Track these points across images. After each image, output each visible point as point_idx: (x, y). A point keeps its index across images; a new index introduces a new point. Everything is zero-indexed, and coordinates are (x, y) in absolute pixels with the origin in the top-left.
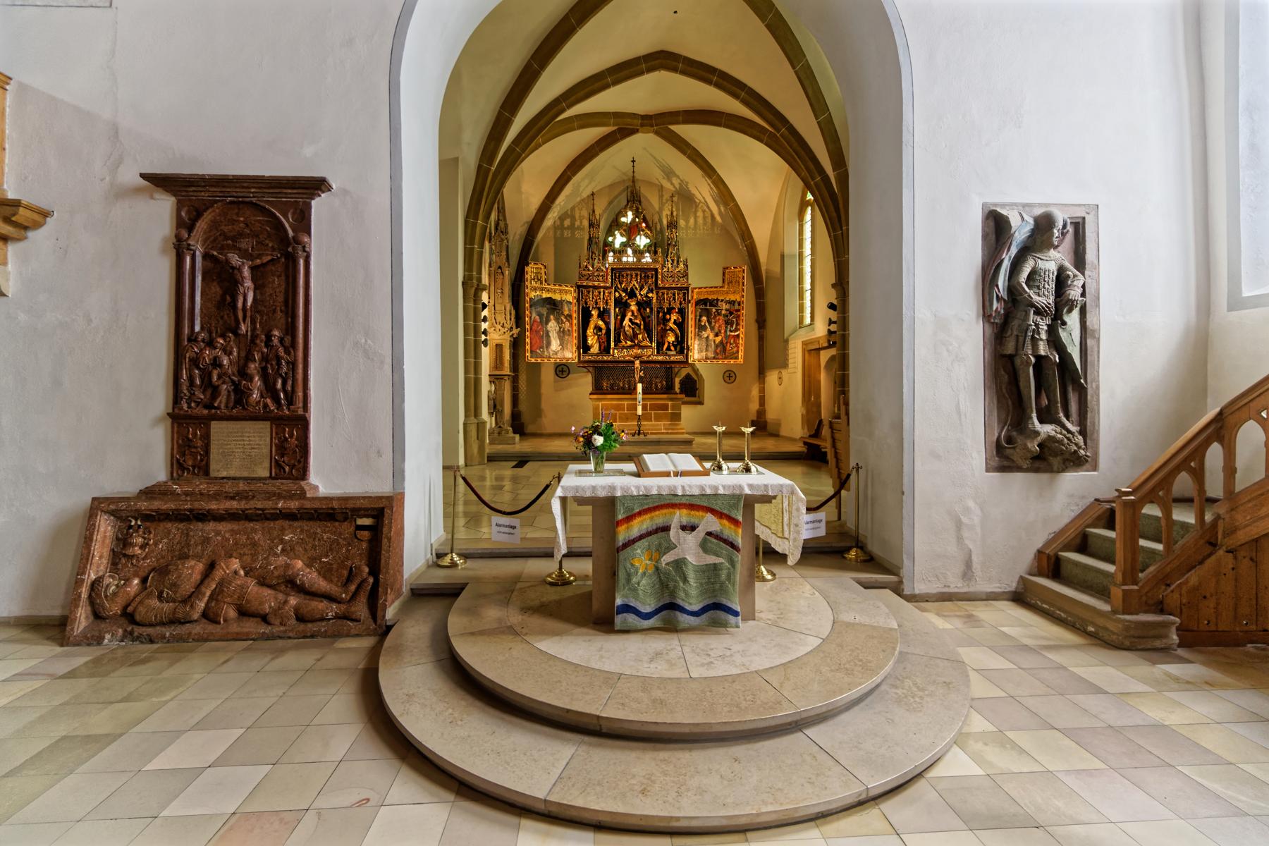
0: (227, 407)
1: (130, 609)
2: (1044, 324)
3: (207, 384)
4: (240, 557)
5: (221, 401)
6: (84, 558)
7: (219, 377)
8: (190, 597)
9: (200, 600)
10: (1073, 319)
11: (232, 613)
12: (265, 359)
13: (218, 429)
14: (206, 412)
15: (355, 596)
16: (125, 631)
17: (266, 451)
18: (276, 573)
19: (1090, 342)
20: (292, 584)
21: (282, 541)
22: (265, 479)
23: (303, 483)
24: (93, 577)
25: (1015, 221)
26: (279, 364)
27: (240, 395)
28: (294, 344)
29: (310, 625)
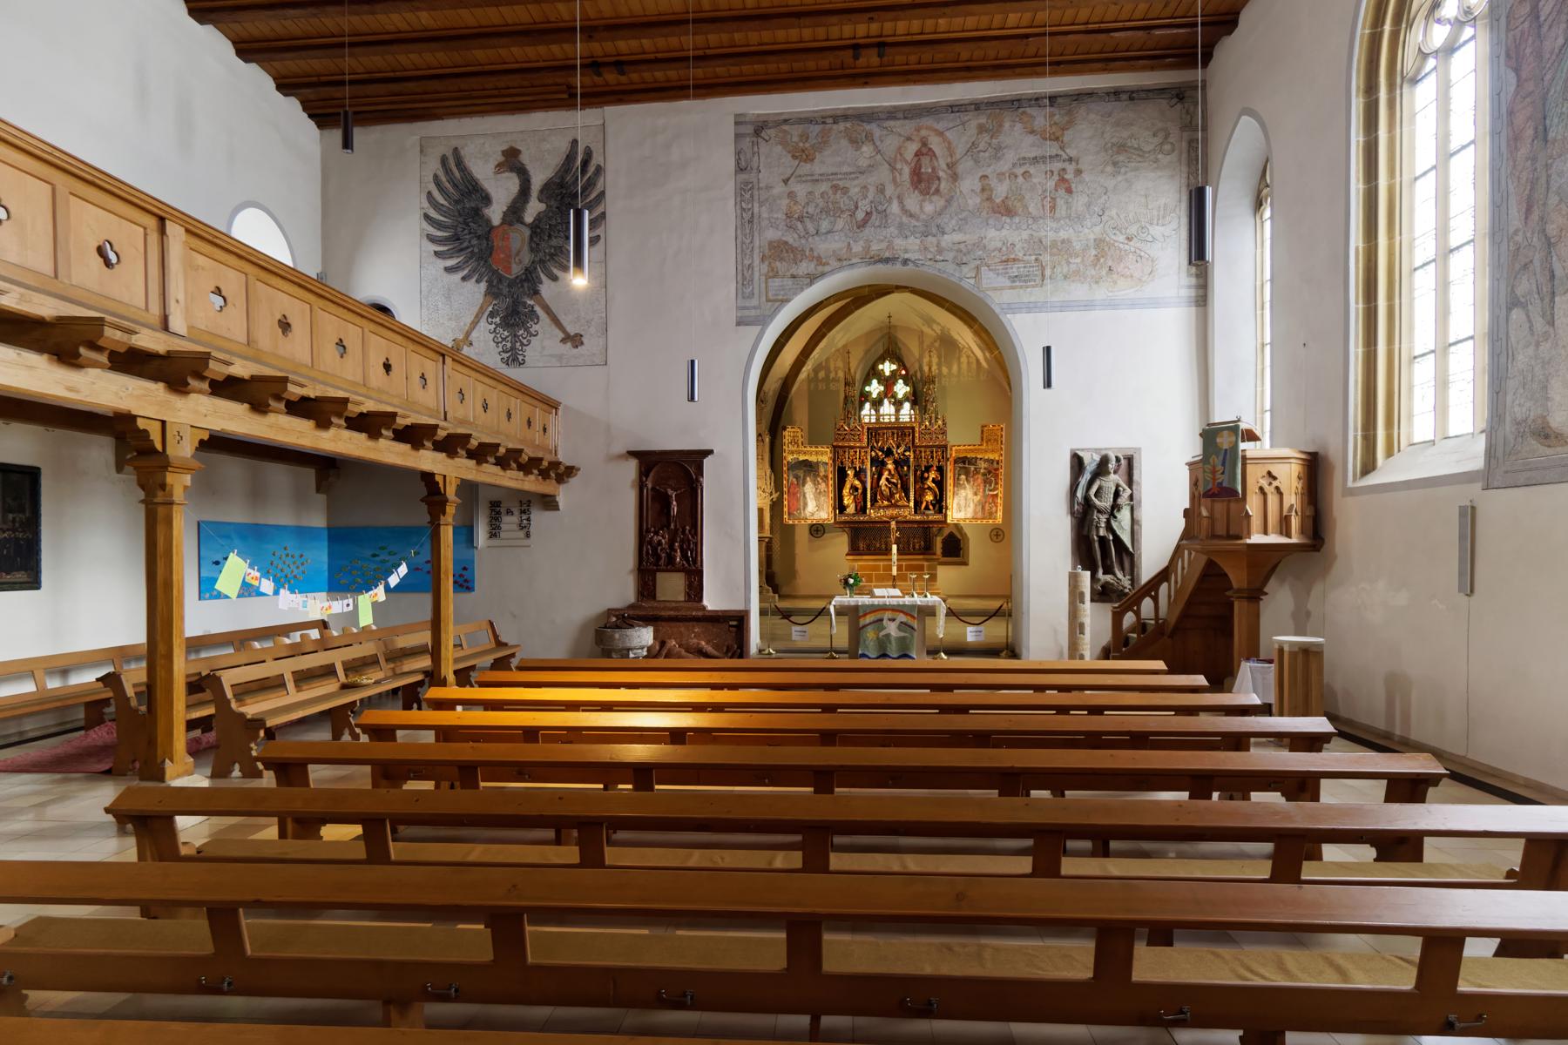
2: (1103, 518)
3: (655, 549)
10: (1124, 516)
12: (682, 541)
13: (660, 576)
25: (1087, 460)
27: (671, 559)
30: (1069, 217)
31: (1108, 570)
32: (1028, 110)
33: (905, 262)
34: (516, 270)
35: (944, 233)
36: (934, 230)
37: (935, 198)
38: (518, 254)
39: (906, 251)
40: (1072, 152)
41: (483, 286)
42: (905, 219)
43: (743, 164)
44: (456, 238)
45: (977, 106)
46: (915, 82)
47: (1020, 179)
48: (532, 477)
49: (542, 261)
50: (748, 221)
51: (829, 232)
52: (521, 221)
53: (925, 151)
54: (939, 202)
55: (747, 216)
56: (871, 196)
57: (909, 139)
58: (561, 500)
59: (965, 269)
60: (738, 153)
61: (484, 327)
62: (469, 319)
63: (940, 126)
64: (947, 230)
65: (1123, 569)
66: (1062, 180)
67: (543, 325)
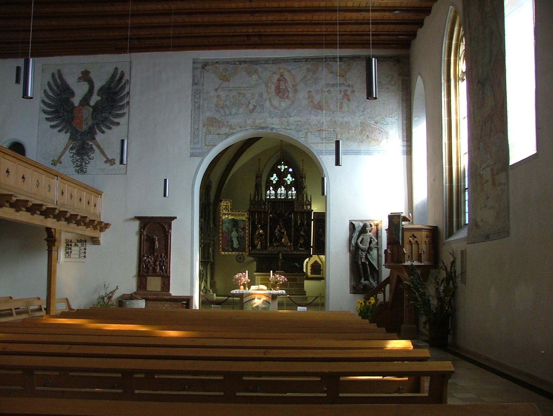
2: (364, 254)
3: (147, 267)
12: (160, 261)
19: (380, 258)
27: (154, 270)
30: (349, 111)
31: (367, 279)
32: (330, 63)
33: (272, 129)
34: (85, 127)
35: (290, 116)
36: (286, 115)
37: (287, 100)
38: (86, 120)
39: (272, 124)
40: (350, 83)
41: (68, 135)
42: (272, 109)
43: (196, 81)
44: (57, 112)
45: (307, 60)
46: (278, 48)
47: (326, 93)
48: (89, 229)
49: (97, 124)
50: (197, 108)
51: (236, 114)
52: (88, 104)
53: (282, 79)
54: (288, 102)
55: (197, 105)
56: (256, 98)
57: (275, 73)
58: (102, 240)
59: (300, 134)
60: (194, 76)
61: (68, 154)
62: (61, 150)
63: (289, 68)
64: (292, 115)
65: (373, 278)
66: (346, 95)
67: (96, 154)
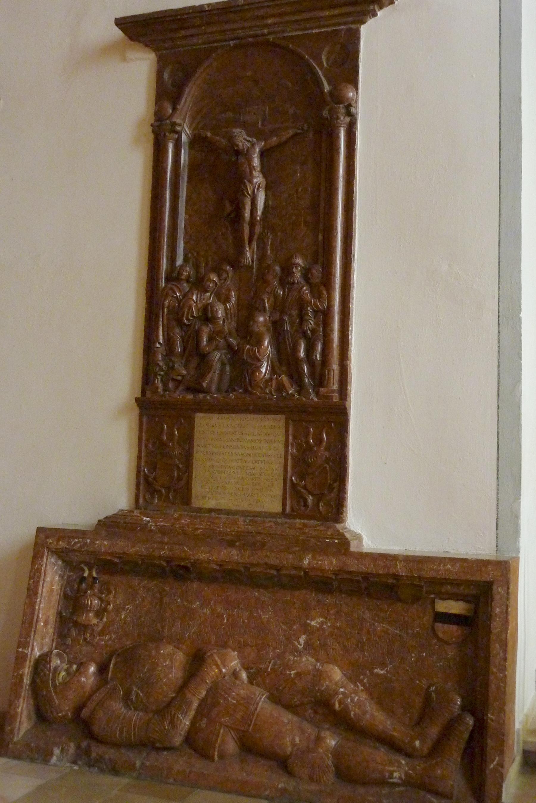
0: (219, 390)
1: (85, 713)
4: (241, 648)
5: (212, 379)
6: (28, 623)
7: (211, 339)
8: (169, 704)
9: (185, 714)
11: (231, 746)
12: (280, 307)
14: (190, 397)
15: (437, 749)
16: (78, 747)
17: (276, 467)
18: (299, 684)
20: (324, 709)
21: (305, 628)
22: (273, 515)
23: (339, 526)
24: (37, 653)
26: (302, 317)
27: (242, 366)
28: (327, 281)
29: (361, 790)
